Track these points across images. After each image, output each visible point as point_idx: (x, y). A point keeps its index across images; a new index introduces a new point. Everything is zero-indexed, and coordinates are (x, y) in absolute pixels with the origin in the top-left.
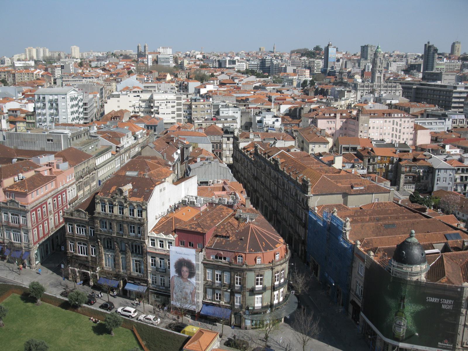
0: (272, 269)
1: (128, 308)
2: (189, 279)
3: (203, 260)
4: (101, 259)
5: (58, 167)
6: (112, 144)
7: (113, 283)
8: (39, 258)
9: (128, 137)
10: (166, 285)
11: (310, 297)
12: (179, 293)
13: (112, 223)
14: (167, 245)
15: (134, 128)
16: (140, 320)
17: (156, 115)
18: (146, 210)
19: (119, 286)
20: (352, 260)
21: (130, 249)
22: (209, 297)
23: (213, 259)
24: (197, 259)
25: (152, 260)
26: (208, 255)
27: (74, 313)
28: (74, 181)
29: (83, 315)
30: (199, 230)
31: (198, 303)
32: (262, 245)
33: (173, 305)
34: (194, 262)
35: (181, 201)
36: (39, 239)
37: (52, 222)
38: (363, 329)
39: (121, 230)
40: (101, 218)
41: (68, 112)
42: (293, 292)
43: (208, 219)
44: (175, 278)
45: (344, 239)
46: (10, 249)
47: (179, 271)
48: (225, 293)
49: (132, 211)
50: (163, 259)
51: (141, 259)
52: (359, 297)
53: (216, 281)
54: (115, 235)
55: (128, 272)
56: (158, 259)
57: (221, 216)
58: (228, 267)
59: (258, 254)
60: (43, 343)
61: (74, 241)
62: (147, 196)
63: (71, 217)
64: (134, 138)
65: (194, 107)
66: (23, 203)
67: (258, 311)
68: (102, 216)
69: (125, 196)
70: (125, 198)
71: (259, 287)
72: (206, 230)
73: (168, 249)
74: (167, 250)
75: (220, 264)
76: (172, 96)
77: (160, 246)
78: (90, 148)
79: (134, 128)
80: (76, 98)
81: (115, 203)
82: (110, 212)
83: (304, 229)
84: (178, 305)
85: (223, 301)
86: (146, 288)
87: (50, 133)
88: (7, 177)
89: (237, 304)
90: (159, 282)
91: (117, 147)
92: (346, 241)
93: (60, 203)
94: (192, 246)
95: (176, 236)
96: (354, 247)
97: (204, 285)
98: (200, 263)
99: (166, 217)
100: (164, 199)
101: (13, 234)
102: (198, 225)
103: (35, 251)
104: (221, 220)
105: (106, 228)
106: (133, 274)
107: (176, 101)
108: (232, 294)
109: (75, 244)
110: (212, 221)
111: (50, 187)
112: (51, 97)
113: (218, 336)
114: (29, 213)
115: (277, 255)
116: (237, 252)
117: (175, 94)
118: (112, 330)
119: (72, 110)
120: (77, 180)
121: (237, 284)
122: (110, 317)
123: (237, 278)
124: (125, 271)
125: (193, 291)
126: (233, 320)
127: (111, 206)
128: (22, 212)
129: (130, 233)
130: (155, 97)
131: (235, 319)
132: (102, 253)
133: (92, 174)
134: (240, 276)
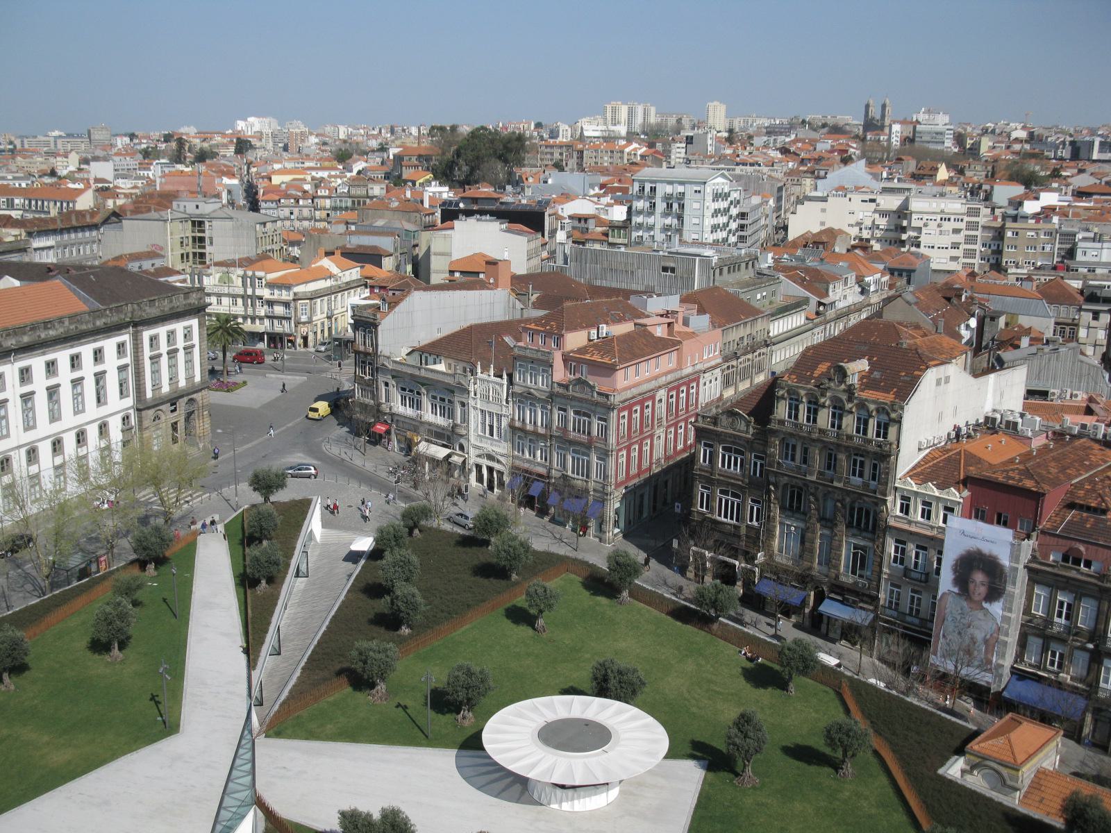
2: (985, 605)
3: (1030, 561)
4: (770, 534)
5: (686, 322)
6: (808, 294)
7: (793, 595)
8: (622, 524)
9: (846, 284)
12: (954, 637)
13: (811, 449)
15: (861, 267)
17: (913, 249)
18: (899, 422)
19: (804, 602)
21: (844, 516)
22: (1031, 658)
23: (1054, 561)
24: (1015, 557)
25: (897, 548)
26: (1043, 549)
27: (703, 633)
28: (719, 360)
29: (722, 642)
30: (1029, 484)
34: (1005, 561)
35: (981, 420)
36: (628, 477)
37: (659, 444)
39: (829, 468)
40: (785, 433)
41: (704, 224)
43: (1053, 464)
44: (950, 599)
46: (560, 494)
47: (962, 580)
48: (1077, 653)
49: (863, 424)
50: (925, 549)
51: (869, 544)
53: (1056, 619)
54: (814, 478)
55: (833, 572)
56: (911, 549)
57: (1087, 463)
58: (1096, 585)
60: (635, 671)
61: (712, 484)
62: (906, 389)
63: (711, 427)
64: (860, 290)
65: (1009, 234)
66: (604, 390)
68: (788, 427)
69: (851, 385)
70: (850, 391)
72: (1046, 487)
73: (941, 524)
75: (1073, 574)
76: (956, 205)
77: (923, 516)
78: (759, 296)
79: (861, 267)
80: (727, 195)
81: (822, 400)
82: (808, 420)
85: (1068, 673)
86: (872, 616)
87: (669, 253)
88: (574, 328)
90: (905, 606)
91: (820, 304)
93: (682, 405)
95: (966, 493)
97: (1022, 625)
98: (1021, 567)
99: (944, 450)
100: (946, 404)
101: (573, 458)
102: (1027, 473)
103: (615, 504)
104: (1087, 472)
105: (793, 459)
106: (843, 579)
107: (966, 219)
109: (713, 492)
110: (1063, 469)
111: (667, 362)
112: (669, 189)
114: (615, 411)
117: (964, 201)
118: (791, 678)
119: (715, 221)
120: (726, 359)
122: (793, 646)
124: (824, 569)
127: (813, 406)
128: (599, 409)
129: (851, 477)
130: (916, 205)
132: (774, 518)
133: (760, 355)
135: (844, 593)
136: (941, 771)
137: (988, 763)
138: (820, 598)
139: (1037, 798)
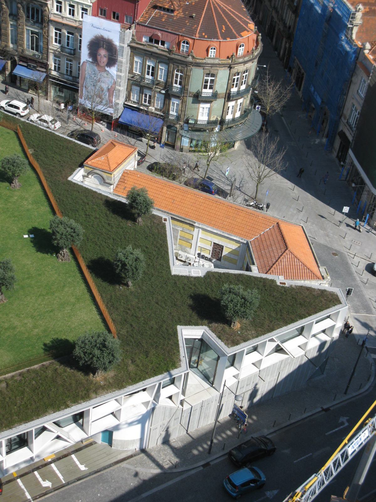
0: (230, 68)
1: (15, 102)
2: (107, 69)
3: (131, 42)
10: (73, 74)
11: (283, 118)
14: (81, 11)
16: (31, 121)
20: (353, 72)
24: (122, 40)
25: (56, 33)
26: (138, 35)
31: (116, 107)
32: (221, 29)
33: (81, 104)
34: (117, 43)
38: (348, 173)
42: (258, 108)
45: (348, 38)
47: (93, 54)
51: (41, 31)
52: (351, 128)
53: (147, 76)
58: (166, 56)
59: (212, 43)
67: (202, 127)
71: (207, 92)
74: (80, 21)
75: (155, 50)
83: (293, 16)
84: (88, 105)
85: (154, 106)
86: (45, 74)
89: (173, 113)
90: (64, 69)
92: (350, 42)
94: (117, 18)
96: (359, 51)
97: (128, 79)
98: (126, 46)
108: (168, 96)
113: (136, 153)
115: (242, 48)
116: (181, 36)
121: (176, 83)
123: (177, 75)
125: (113, 86)
126: (165, 135)
131: (168, 134)
134: (181, 72)
135: (27, 61)
136: (70, 179)
137: (96, 171)
138: (14, 65)
139: (123, 187)
